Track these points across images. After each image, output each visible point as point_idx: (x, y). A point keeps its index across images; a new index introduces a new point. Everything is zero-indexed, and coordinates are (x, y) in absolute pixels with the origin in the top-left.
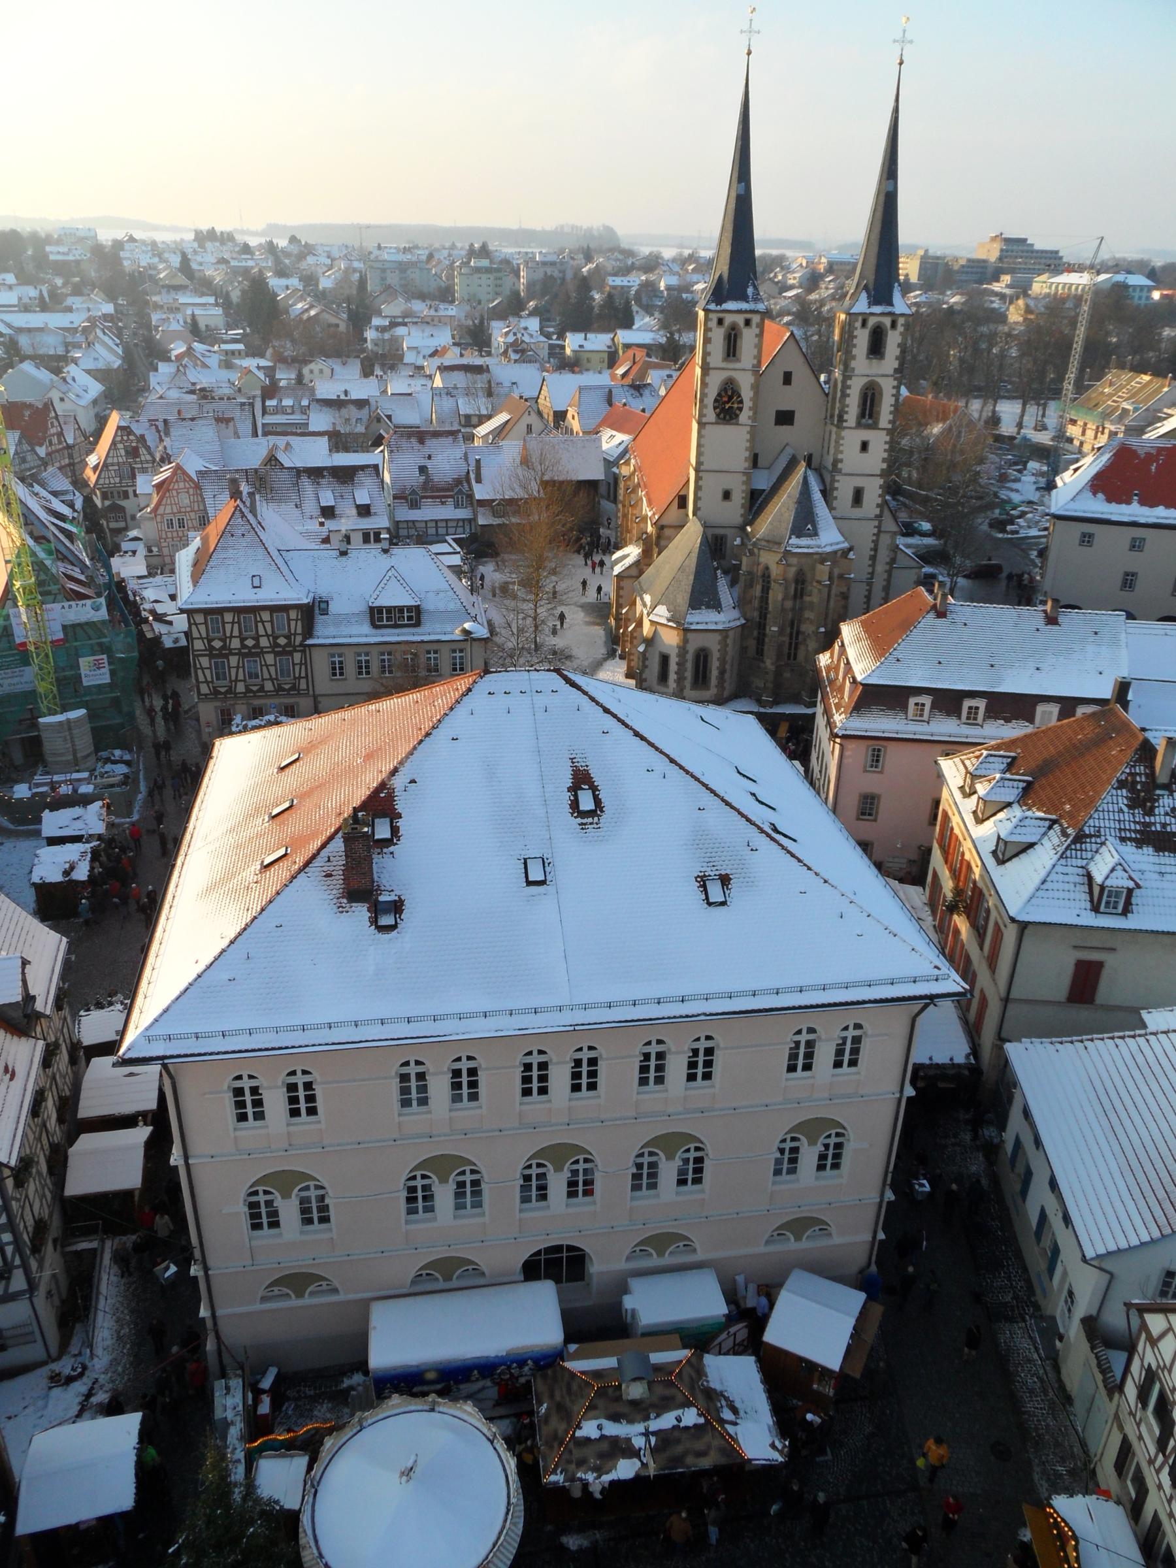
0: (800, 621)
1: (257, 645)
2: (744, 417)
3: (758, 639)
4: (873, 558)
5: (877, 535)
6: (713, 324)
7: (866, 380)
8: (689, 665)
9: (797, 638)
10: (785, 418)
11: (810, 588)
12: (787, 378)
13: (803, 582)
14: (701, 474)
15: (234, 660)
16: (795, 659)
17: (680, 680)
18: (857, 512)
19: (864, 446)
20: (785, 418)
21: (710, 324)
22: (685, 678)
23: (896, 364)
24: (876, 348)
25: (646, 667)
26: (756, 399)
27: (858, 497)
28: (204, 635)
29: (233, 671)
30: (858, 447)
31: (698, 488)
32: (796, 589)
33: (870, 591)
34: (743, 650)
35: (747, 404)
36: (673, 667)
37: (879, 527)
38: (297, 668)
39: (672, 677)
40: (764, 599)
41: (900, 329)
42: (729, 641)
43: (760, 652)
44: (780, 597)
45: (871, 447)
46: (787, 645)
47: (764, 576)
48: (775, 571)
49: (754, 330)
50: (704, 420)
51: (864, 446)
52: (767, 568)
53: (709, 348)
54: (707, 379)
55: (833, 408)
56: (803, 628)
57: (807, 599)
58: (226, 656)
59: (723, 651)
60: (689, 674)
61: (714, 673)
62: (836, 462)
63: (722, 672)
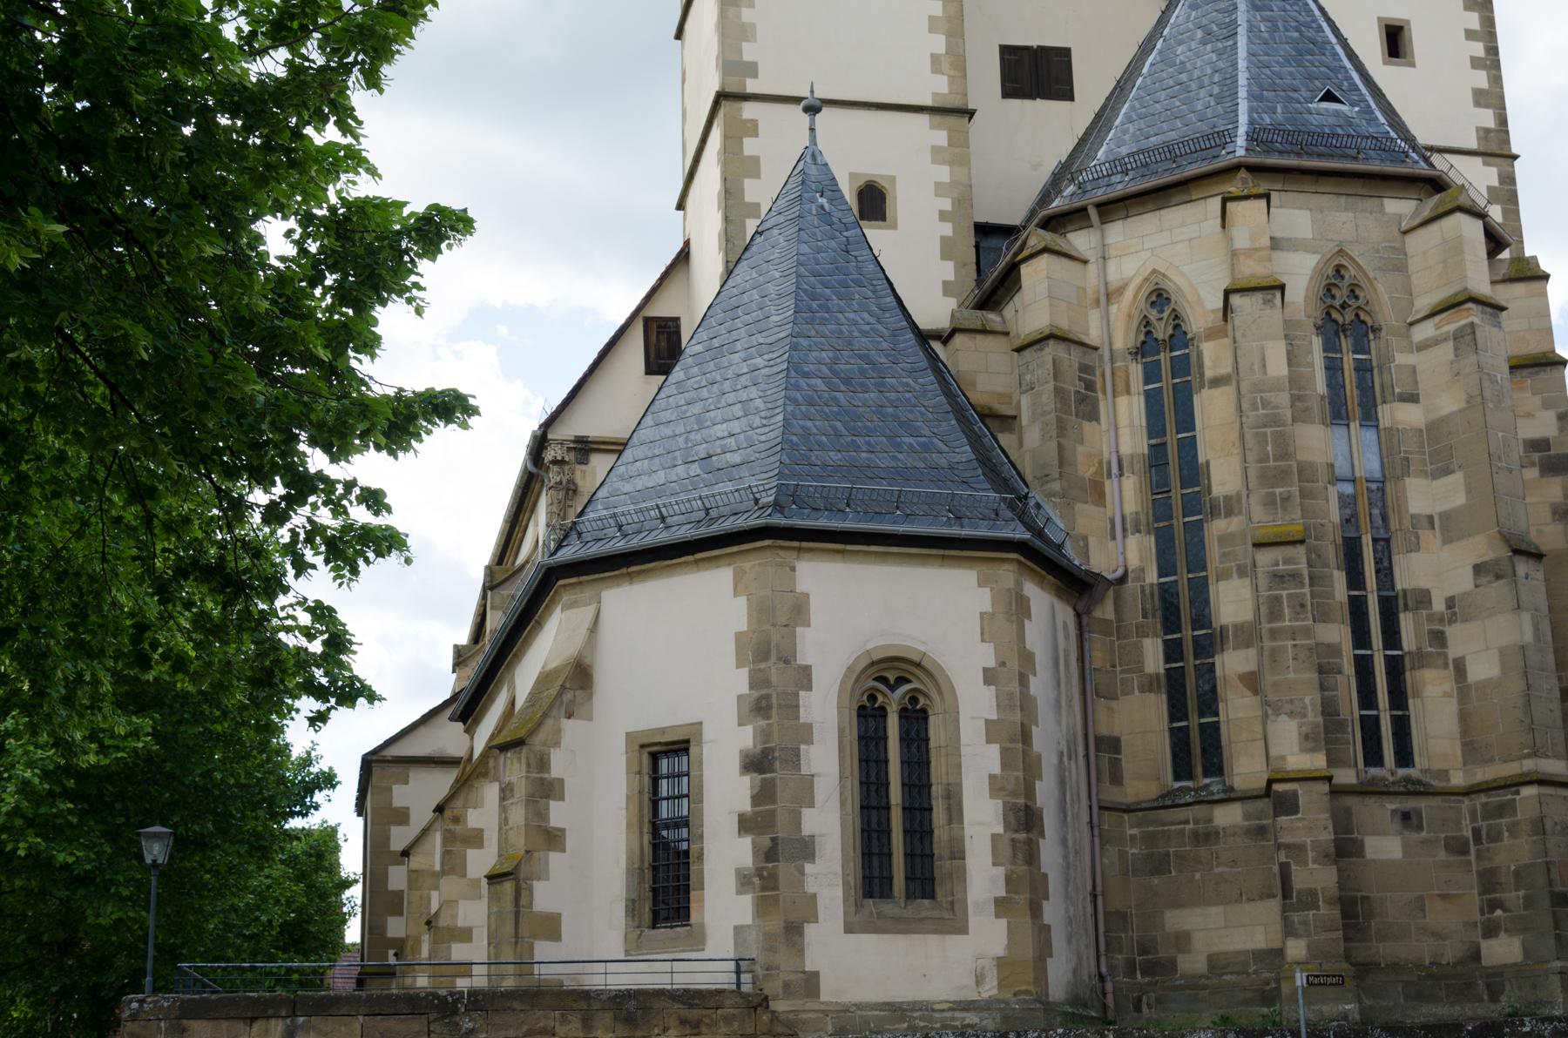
0: (1384, 545)
3: (1174, 684)
8: (826, 760)
9: (1392, 636)
11: (1401, 359)
14: (749, 110)
16: (1404, 756)
22: (806, 849)
25: (554, 839)
32: (1333, 368)
34: (1103, 751)
36: (723, 790)
39: (724, 854)
40: (1172, 464)
45: (1419, 40)
46: (1349, 668)
47: (1145, 348)
52: (1159, 297)
56: (1412, 571)
59: (1010, 674)
60: (827, 820)
61: (980, 819)
63: (1024, 819)
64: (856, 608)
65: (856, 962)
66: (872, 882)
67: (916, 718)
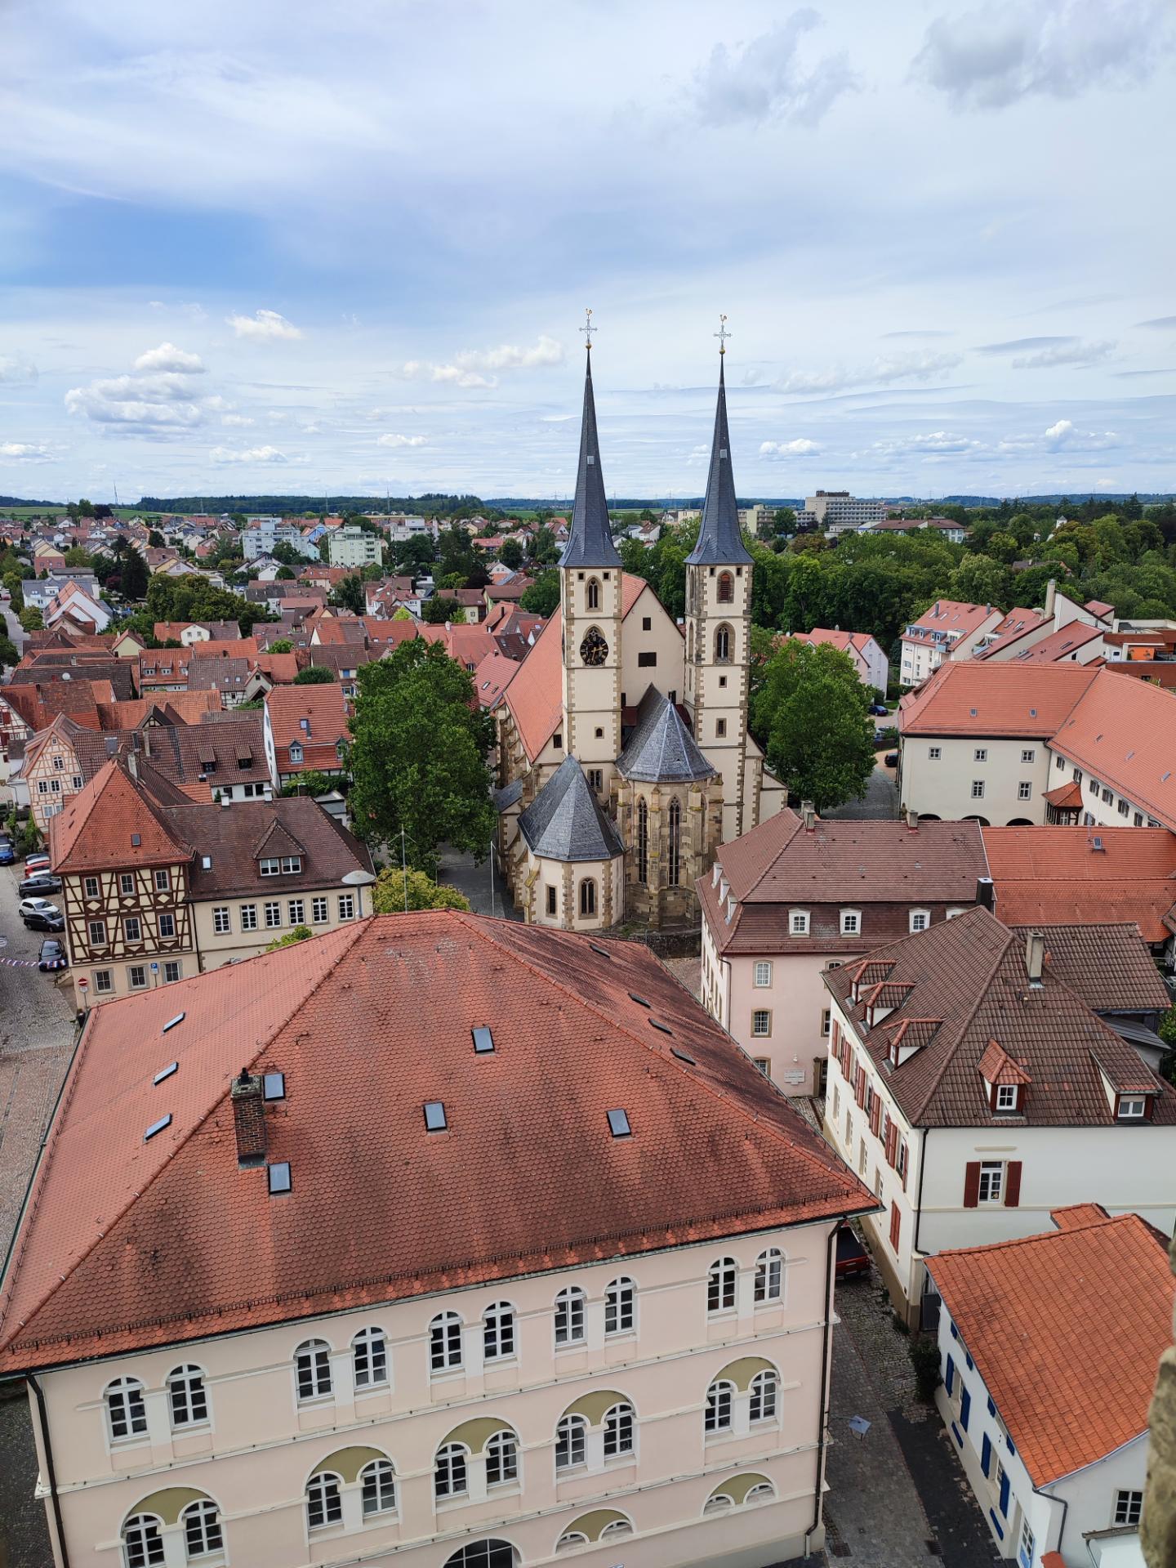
1: (137, 905)
2: (610, 660)
4: (741, 782)
5: (743, 761)
6: (574, 578)
7: (718, 622)
10: (648, 660)
12: (647, 624)
13: (678, 809)
15: (112, 921)
17: (568, 909)
18: (721, 742)
19: (723, 681)
20: (648, 660)
21: (571, 579)
23: (744, 607)
24: (725, 594)
26: (619, 644)
27: (721, 726)
28: (80, 898)
29: (111, 933)
30: (718, 682)
31: (571, 728)
33: (741, 814)
34: (627, 876)
35: (612, 649)
36: (560, 899)
37: (743, 754)
38: (180, 925)
39: (560, 907)
40: (642, 829)
41: (745, 575)
42: (613, 869)
43: (643, 878)
44: (658, 825)
48: (651, 800)
49: (613, 582)
50: (573, 665)
51: (723, 681)
53: (572, 600)
54: (573, 628)
55: (691, 648)
56: (682, 852)
57: (682, 825)
58: (104, 918)
59: (608, 880)
60: (576, 904)
61: (600, 902)
62: (697, 698)
63: (608, 900)
64: (581, 871)
65: (581, 924)
66: (583, 910)
67: (591, 886)
